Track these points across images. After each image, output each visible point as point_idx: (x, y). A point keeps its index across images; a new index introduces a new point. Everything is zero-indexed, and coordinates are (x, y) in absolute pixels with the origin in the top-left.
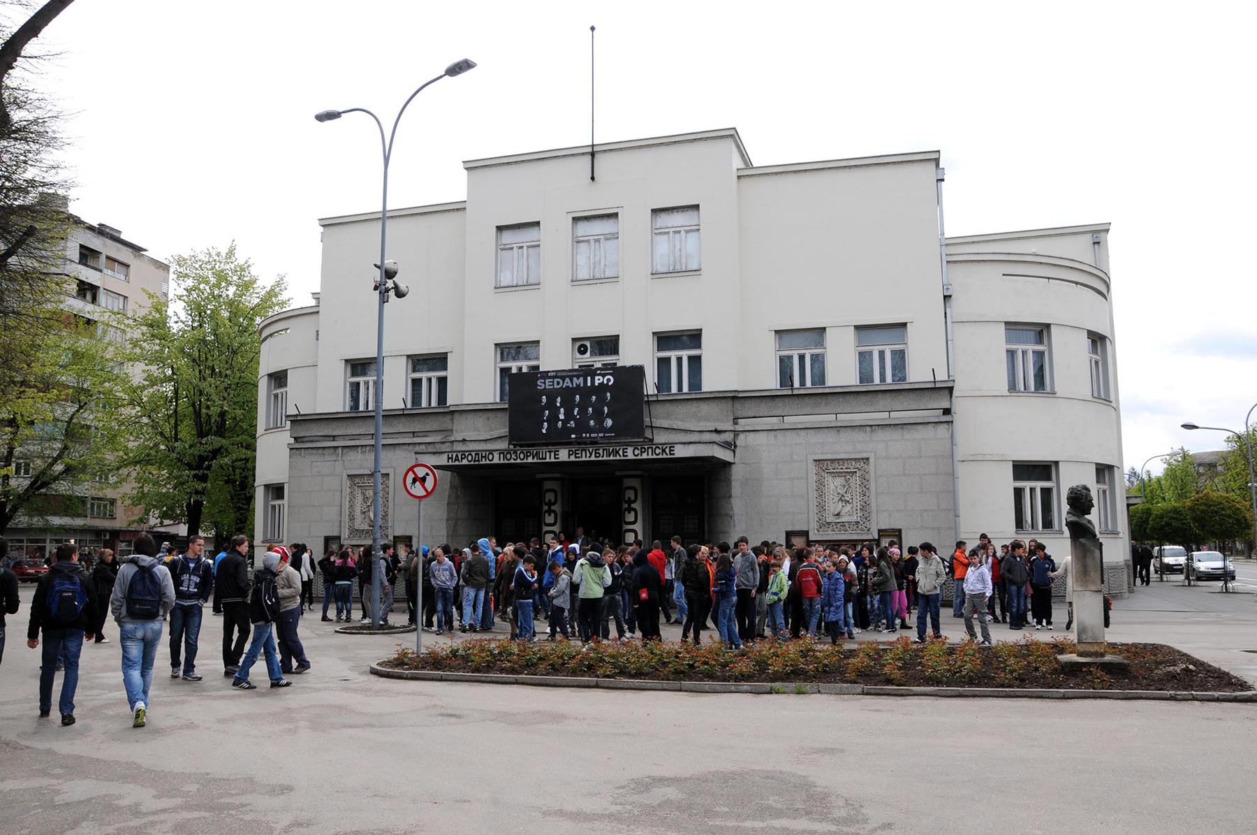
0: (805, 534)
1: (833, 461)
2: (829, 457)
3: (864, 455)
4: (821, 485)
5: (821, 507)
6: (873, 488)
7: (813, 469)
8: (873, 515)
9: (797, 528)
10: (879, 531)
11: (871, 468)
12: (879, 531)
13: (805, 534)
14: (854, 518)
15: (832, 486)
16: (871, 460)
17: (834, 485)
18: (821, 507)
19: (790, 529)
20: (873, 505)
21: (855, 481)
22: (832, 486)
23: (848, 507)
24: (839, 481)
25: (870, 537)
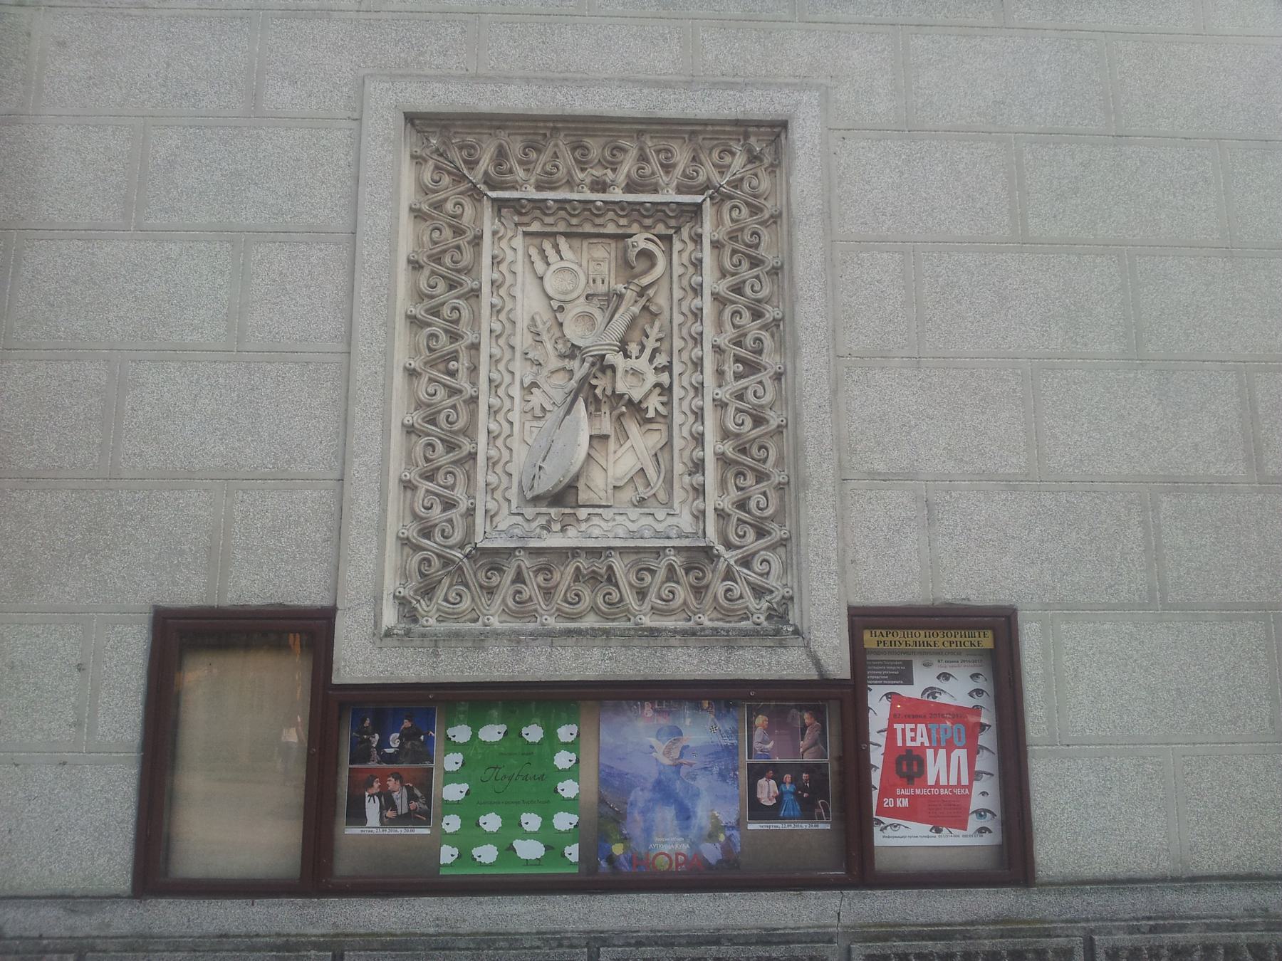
0: (310, 631)
1: (537, 129)
2: (516, 99)
3: (756, 105)
4: (447, 274)
5: (444, 441)
6: (810, 313)
7: (398, 179)
8: (817, 518)
9: (250, 586)
10: (862, 620)
11: (804, 180)
12: (862, 620)
13: (310, 631)
14: (677, 522)
15: (528, 304)
16: (805, 137)
17: (537, 288)
18: (444, 441)
19: (190, 591)
20: (815, 428)
21: (690, 273)
22: (528, 304)
23: (633, 452)
24: (579, 269)
25: (787, 664)
